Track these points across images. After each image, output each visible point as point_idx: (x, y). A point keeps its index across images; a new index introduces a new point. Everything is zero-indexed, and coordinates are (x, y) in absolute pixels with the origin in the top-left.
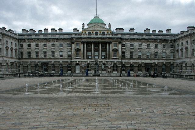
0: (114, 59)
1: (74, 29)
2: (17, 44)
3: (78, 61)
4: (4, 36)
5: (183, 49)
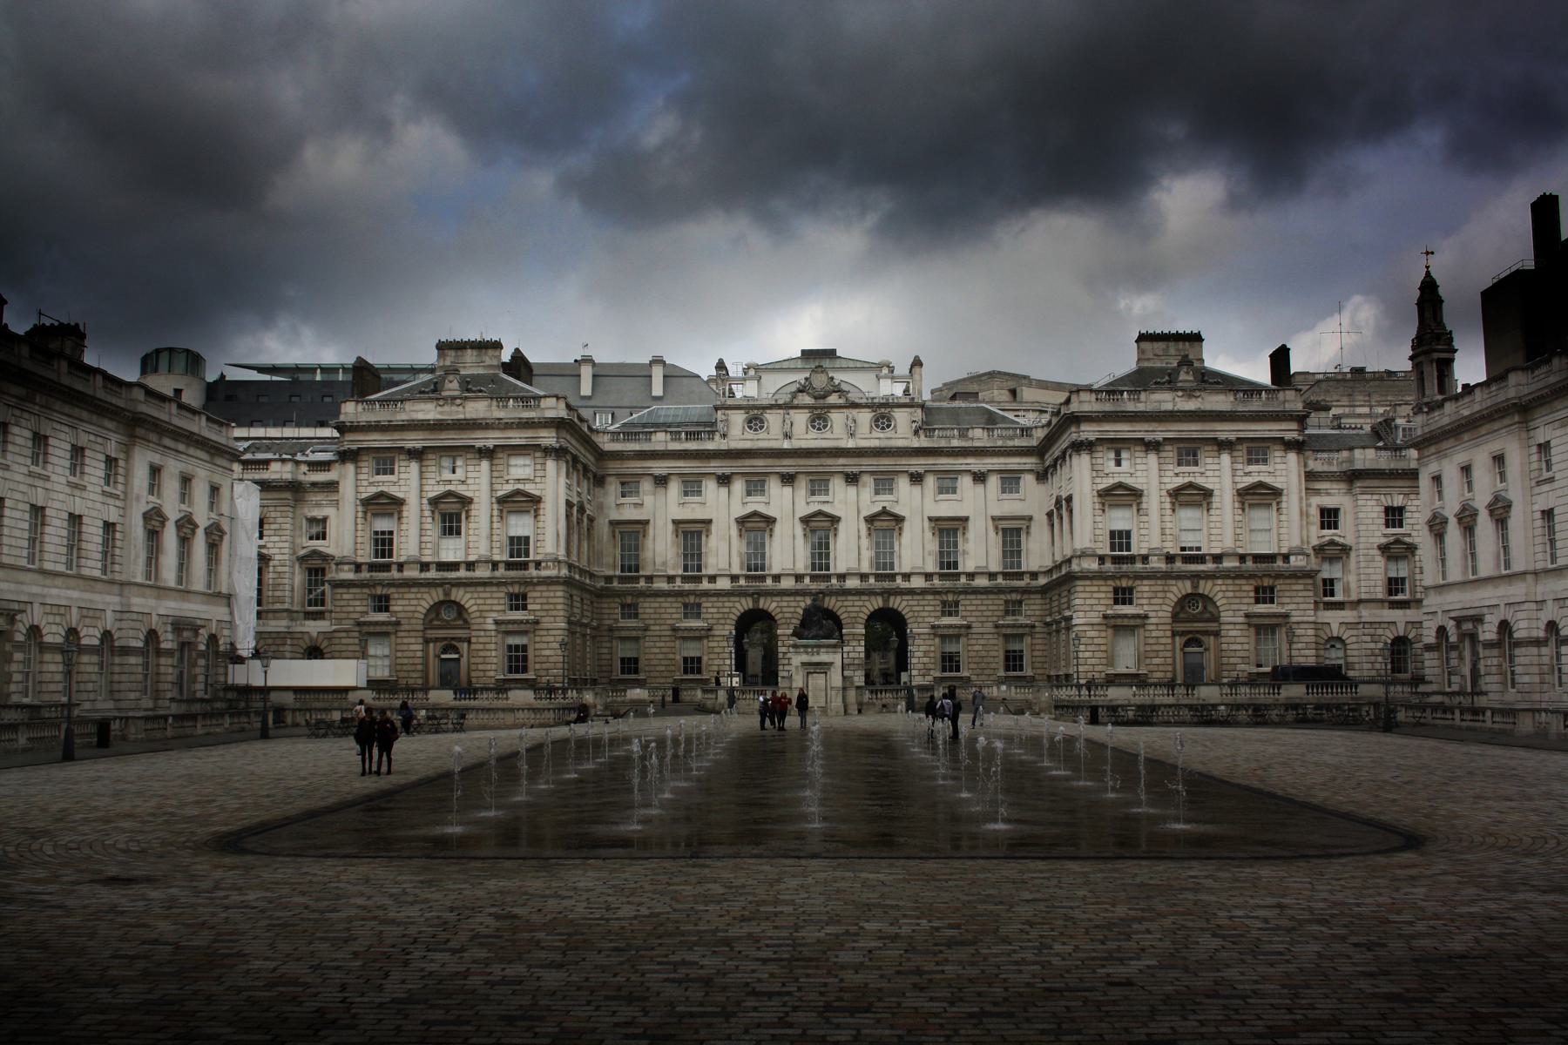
5: (1474, 514)
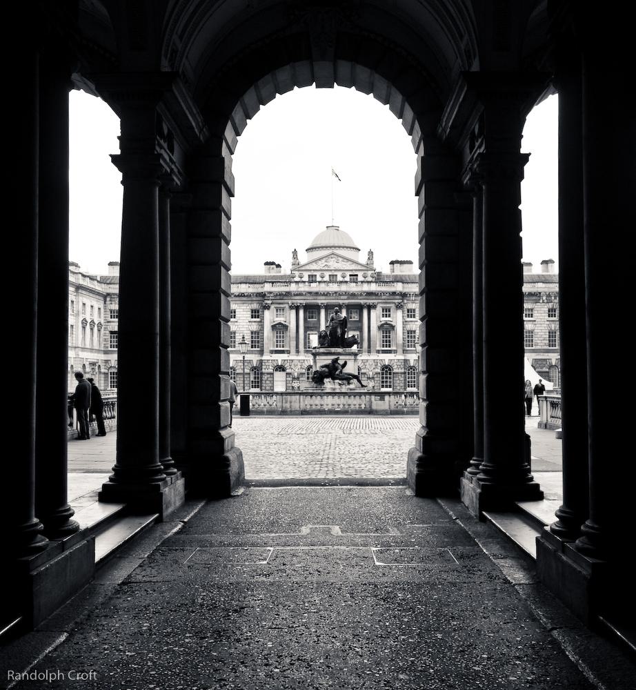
0: (384, 352)
1: (267, 264)
2: (102, 310)
3: (280, 358)
4: (80, 291)
